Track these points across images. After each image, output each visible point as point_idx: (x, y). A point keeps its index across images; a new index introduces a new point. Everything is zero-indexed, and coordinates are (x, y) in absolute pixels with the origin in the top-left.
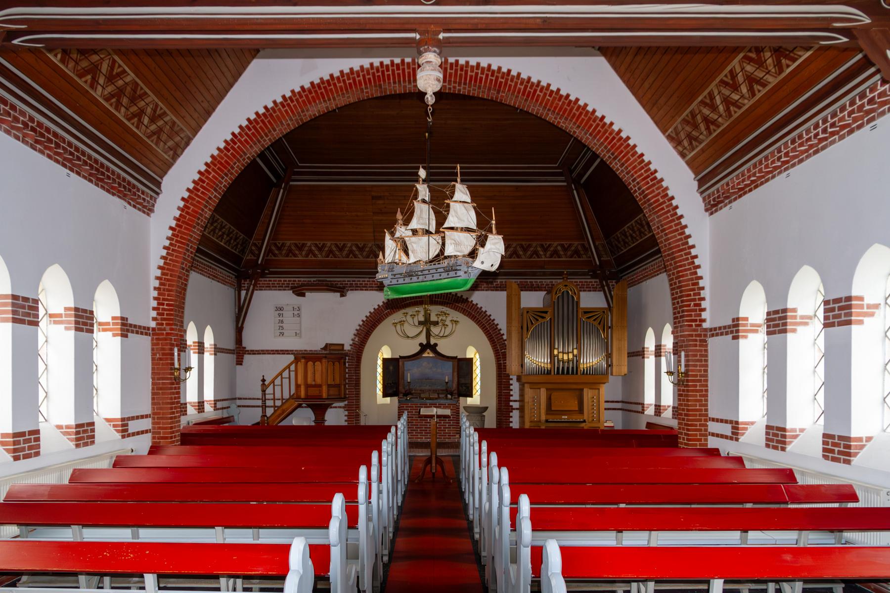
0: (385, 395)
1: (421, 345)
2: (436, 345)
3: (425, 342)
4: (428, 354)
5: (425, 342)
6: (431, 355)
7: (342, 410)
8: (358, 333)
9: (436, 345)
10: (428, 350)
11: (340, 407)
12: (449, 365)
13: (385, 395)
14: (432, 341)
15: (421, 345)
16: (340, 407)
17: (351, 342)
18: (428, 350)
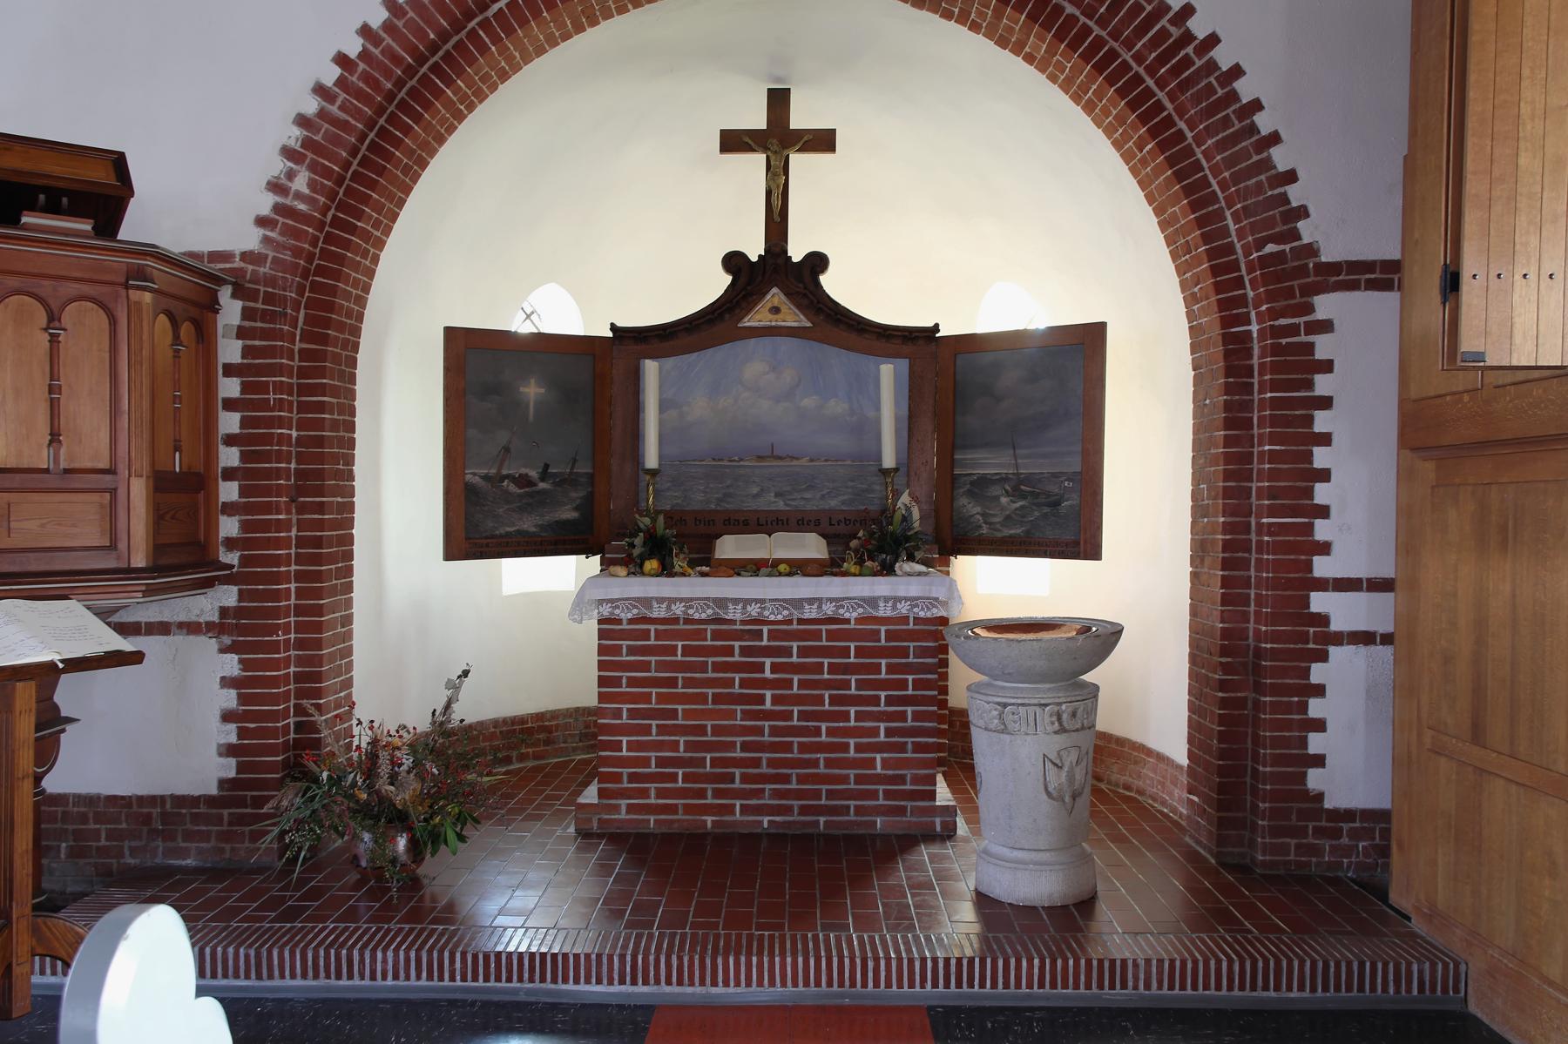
0: (475, 529)
1: (734, 262)
2: (817, 262)
3: (755, 249)
4: (774, 310)
5: (755, 249)
6: (792, 317)
7: (209, 644)
8: (313, 145)
9: (817, 262)
10: (775, 296)
11: (192, 628)
12: (889, 374)
13: (475, 529)
14: (796, 252)
15: (734, 262)
16: (192, 628)
17: (265, 203)
18: (775, 296)
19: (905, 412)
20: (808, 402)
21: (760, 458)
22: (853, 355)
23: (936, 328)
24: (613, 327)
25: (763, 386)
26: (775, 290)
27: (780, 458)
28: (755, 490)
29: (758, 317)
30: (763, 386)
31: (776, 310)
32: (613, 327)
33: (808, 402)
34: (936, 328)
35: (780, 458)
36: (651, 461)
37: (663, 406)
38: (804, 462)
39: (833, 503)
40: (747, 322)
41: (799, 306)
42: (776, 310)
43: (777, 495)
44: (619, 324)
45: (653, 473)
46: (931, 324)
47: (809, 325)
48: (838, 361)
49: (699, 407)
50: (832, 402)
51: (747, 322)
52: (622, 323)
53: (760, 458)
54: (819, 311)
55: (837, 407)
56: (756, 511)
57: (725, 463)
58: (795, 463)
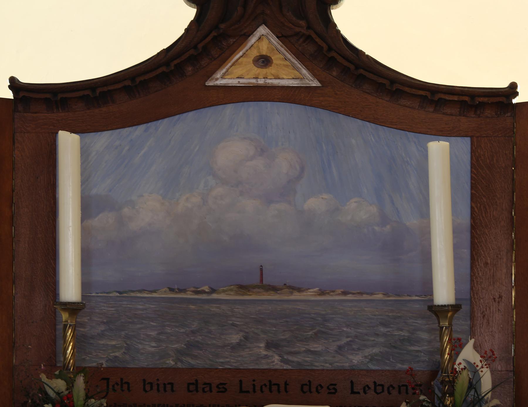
6: (289, 73)
12: (441, 157)
18: (263, 39)
19: (466, 220)
20: (317, 203)
21: (243, 288)
22: (384, 132)
23: (512, 90)
24: (14, 84)
25: (247, 179)
26: (263, 30)
27: (274, 289)
28: (235, 338)
29: (237, 72)
30: (247, 179)
31: (264, 61)
32: (14, 84)
33: (317, 203)
34: (512, 90)
35: (274, 289)
36: (70, 289)
37: (88, 208)
38: (309, 295)
39: (356, 359)
40: (220, 79)
41: (300, 56)
42: (264, 61)
43: (269, 346)
44: (25, 79)
45: (73, 308)
46: (504, 84)
47: (315, 83)
48: (360, 141)
49: (147, 209)
50: (352, 204)
51: (220, 79)
52: (26, 78)
53: (243, 288)
54: (331, 63)
55: (360, 211)
56: (237, 370)
57: (189, 295)
58: (296, 296)
